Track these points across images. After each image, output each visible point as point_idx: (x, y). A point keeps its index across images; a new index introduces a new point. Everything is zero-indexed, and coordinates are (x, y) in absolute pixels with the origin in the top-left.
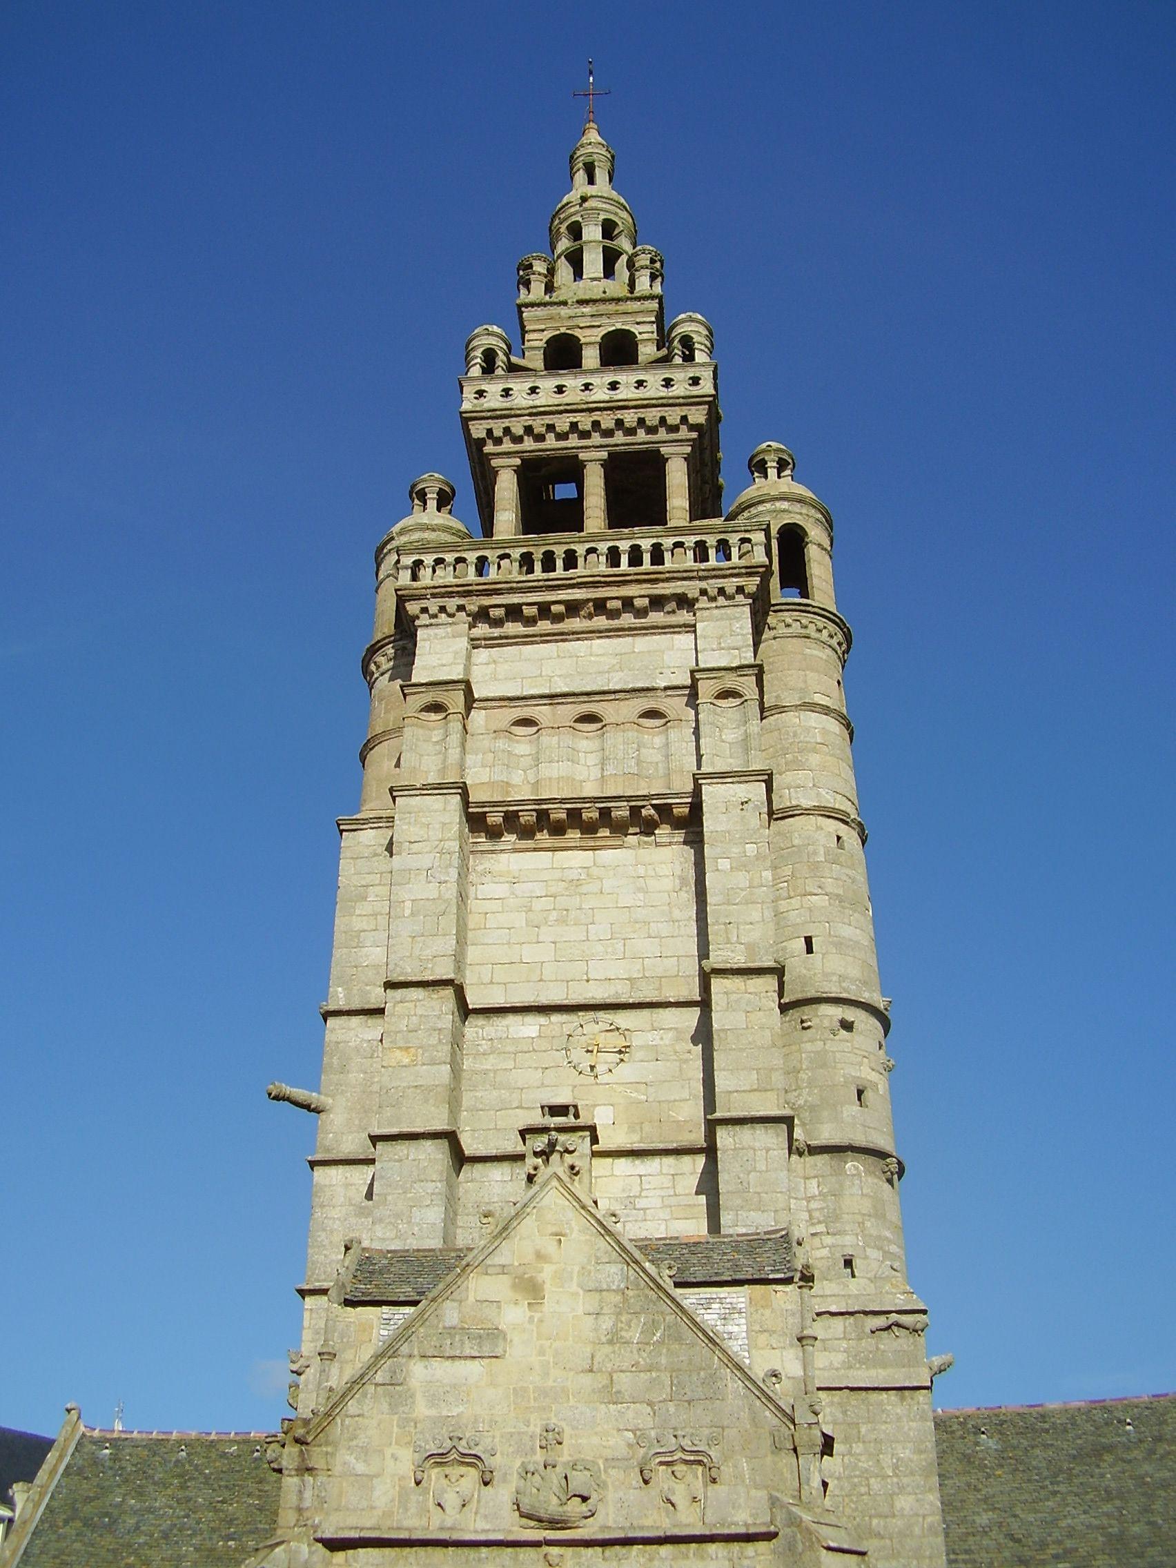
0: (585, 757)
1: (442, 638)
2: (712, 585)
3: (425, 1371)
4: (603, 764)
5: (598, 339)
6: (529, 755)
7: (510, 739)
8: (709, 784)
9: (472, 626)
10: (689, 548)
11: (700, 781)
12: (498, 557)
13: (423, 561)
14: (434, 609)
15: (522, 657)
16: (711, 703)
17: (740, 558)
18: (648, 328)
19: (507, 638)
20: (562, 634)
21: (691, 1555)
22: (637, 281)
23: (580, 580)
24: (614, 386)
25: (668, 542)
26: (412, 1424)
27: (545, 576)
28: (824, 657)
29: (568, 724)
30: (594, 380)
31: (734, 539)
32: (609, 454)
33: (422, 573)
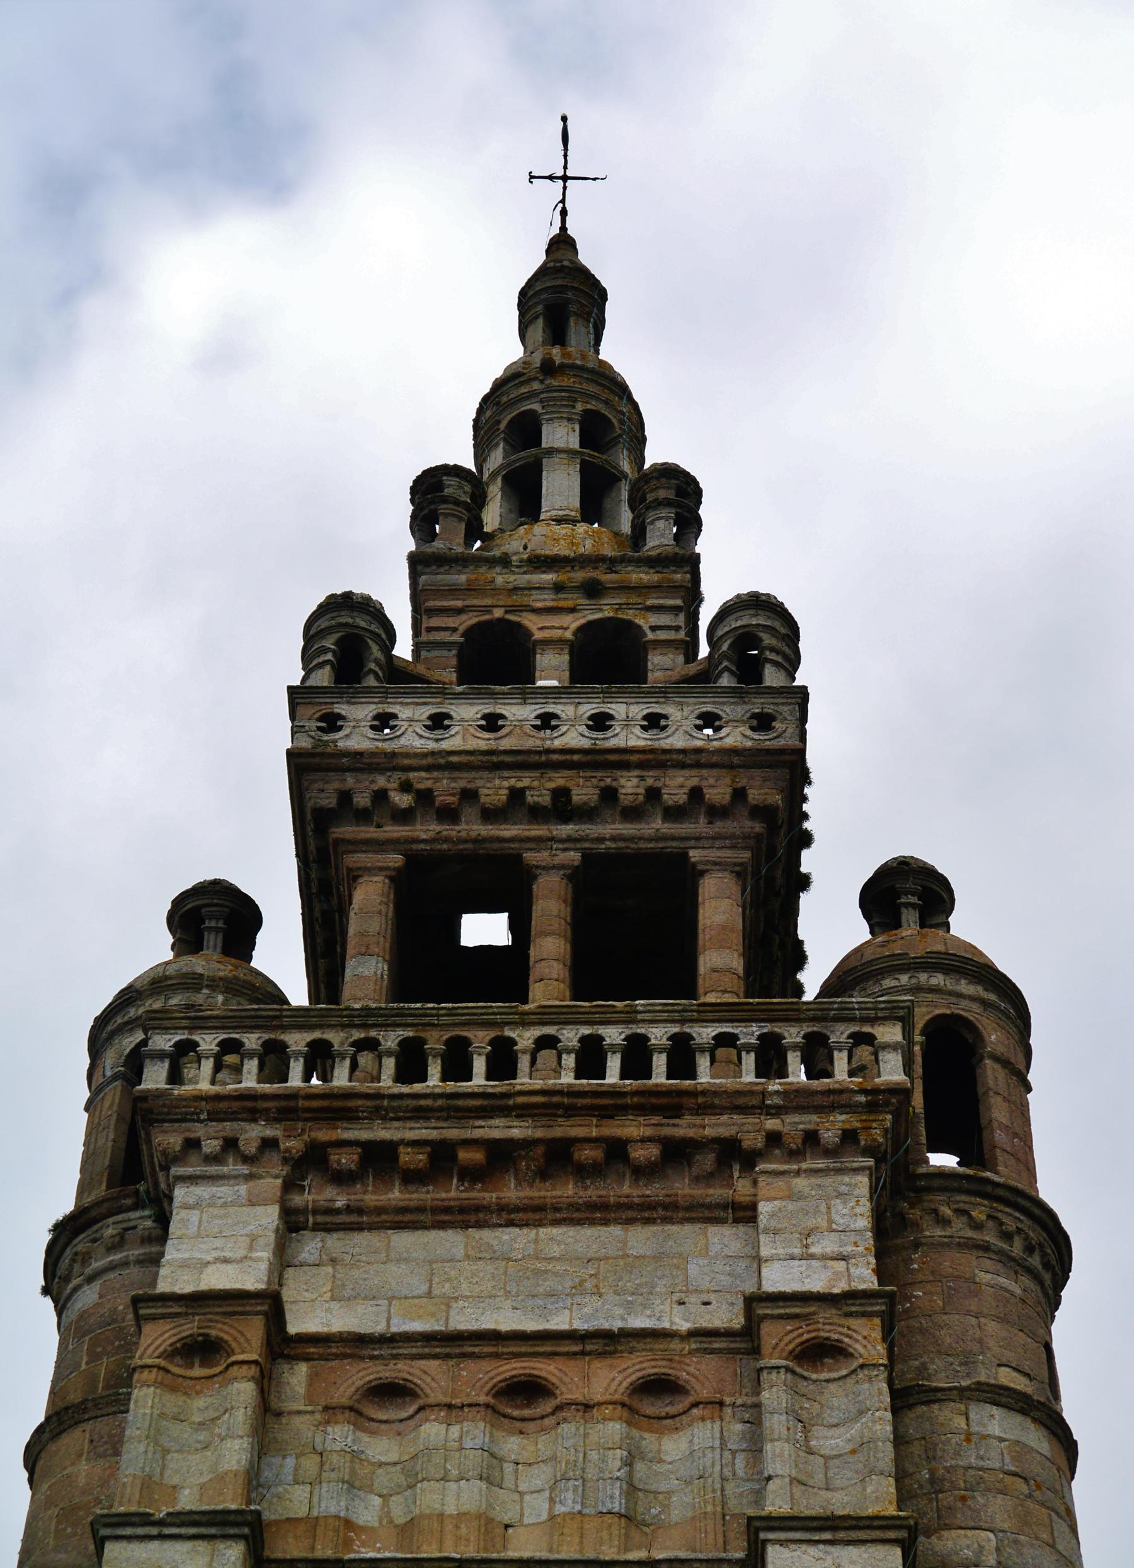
0: (516, 1471)
1: (225, 1205)
2: (792, 1125)
4: (552, 1489)
5: (568, 635)
6: (395, 1464)
7: (357, 1427)
8: (782, 1543)
9: (290, 1185)
10: (748, 1048)
11: (763, 1535)
12: (353, 1045)
13: (197, 1044)
14: (211, 1146)
15: (393, 1255)
16: (788, 1369)
17: (851, 1074)
18: (665, 619)
19: (360, 1211)
20: (478, 1209)
22: (649, 528)
23: (520, 1100)
24: (600, 722)
25: (705, 1033)
27: (451, 1086)
28: (1018, 1292)
29: (482, 1399)
30: (564, 709)
31: (840, 1034)
32: (584, 856)
33: (189, 1072)
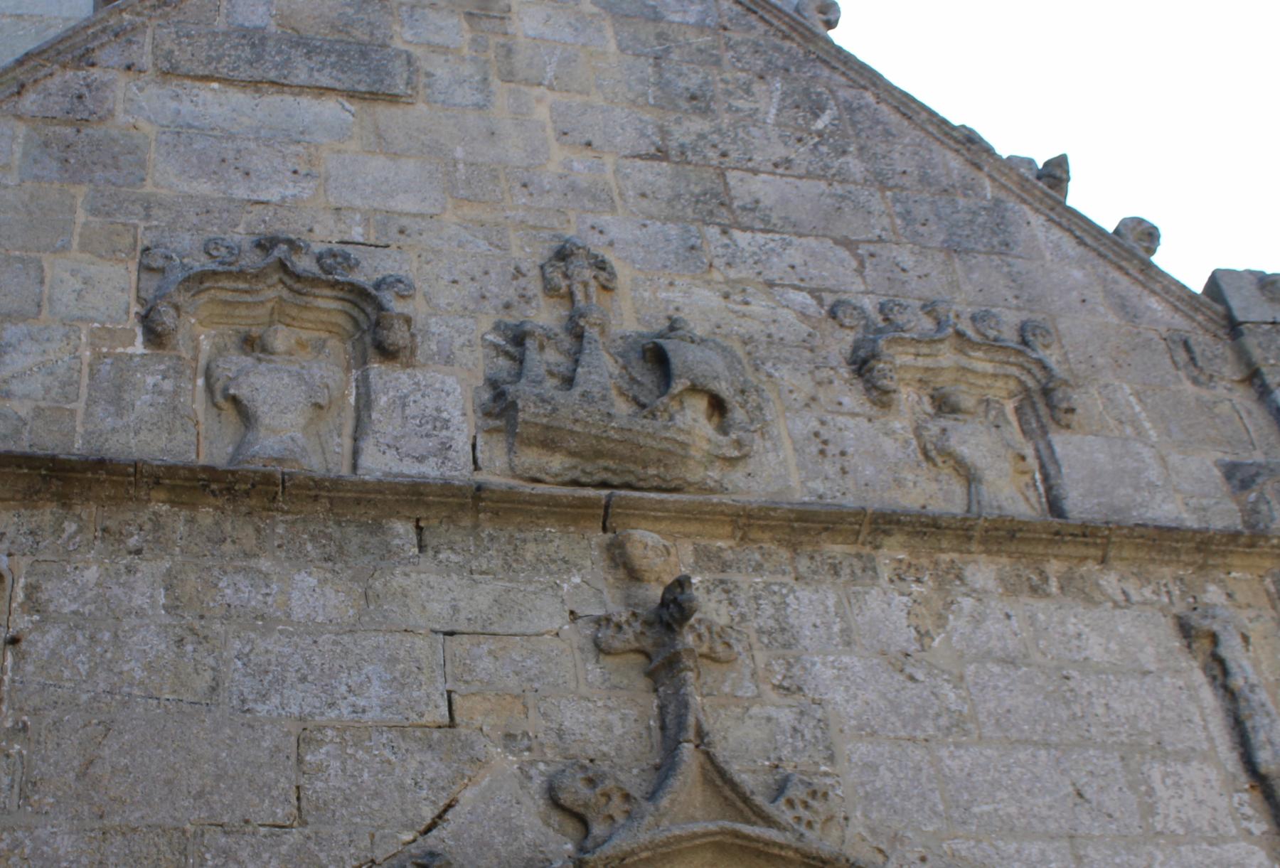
3: (173, 105)
21: (1054, 587)
26: (138, 208)
